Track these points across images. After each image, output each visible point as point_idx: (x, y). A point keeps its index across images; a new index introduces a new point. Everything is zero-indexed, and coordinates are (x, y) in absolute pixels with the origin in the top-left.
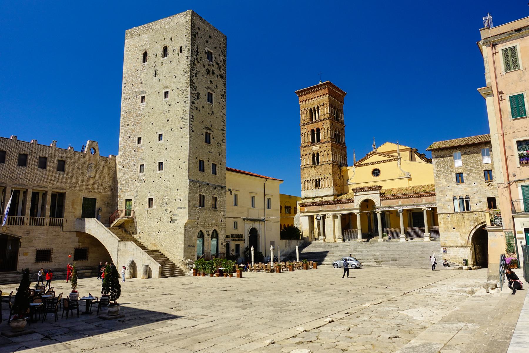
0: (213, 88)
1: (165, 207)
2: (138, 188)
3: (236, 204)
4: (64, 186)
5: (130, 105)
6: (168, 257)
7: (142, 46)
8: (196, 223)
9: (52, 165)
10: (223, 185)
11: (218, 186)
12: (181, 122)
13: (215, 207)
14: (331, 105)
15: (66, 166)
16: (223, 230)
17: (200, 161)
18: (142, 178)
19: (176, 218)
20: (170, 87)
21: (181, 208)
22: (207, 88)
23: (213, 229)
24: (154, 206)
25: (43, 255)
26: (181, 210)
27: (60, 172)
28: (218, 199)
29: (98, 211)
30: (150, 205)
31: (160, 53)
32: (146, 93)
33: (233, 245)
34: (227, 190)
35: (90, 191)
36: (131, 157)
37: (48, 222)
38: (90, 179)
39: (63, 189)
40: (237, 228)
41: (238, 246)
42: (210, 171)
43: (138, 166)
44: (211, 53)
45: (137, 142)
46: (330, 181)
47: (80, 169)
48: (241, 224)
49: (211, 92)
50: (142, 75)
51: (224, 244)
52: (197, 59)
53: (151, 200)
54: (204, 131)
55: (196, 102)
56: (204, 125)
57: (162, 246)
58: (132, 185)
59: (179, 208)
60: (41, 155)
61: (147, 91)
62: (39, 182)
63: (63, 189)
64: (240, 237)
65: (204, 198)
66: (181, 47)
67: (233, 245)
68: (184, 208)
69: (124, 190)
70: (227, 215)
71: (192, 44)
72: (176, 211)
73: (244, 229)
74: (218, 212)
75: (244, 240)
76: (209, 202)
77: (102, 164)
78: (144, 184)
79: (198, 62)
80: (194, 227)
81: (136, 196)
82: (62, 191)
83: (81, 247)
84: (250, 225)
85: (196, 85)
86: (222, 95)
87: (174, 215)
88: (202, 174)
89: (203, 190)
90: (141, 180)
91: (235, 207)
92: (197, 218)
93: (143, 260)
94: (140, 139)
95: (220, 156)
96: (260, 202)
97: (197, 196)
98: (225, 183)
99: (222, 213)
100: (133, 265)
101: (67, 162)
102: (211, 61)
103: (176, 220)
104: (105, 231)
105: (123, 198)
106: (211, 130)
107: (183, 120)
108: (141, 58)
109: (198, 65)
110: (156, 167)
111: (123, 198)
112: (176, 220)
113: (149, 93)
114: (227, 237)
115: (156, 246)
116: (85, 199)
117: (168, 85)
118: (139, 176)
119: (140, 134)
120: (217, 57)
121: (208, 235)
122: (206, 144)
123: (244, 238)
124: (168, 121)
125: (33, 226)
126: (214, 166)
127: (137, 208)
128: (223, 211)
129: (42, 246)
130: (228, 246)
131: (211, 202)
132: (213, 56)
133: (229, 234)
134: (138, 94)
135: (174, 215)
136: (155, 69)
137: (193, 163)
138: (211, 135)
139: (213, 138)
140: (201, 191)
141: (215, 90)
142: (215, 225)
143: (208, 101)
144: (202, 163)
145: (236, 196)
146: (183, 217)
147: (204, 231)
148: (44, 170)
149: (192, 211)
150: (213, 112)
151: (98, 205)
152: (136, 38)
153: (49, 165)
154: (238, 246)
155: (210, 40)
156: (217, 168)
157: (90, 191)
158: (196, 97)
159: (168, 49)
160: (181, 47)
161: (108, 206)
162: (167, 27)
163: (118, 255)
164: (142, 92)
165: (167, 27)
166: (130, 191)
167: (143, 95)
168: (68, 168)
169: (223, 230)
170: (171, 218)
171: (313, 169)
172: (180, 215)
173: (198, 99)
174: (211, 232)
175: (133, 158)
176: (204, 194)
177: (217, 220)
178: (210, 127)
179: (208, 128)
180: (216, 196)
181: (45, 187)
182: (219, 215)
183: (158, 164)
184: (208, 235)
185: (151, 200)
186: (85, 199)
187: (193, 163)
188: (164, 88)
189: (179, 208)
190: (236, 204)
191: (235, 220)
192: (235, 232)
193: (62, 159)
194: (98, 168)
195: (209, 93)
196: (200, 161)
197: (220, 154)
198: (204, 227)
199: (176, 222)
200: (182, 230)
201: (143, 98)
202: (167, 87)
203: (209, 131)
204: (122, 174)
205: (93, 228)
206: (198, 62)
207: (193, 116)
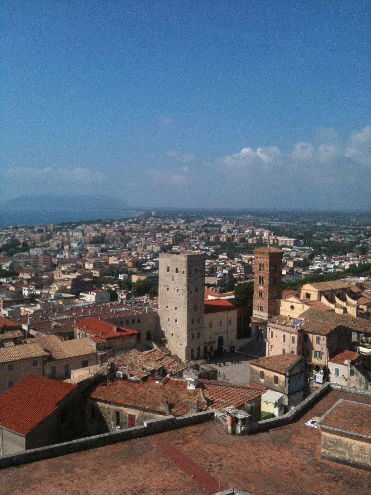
2: (167, 327)
13: (198, 336)
14: (271, 264)
31: (175, 270)
33: (209, 347)
41: (211, 347)
46: (267, 309)
64: (213, 342)
67: (209, 347)
71: (188, 271)
72: (183, 341)
73: (216, 339)
76: (196, 336)
84: (218, 337)
96: (225, 323)
97: (191, 335)
133: (207, 342)
144: (193, 320)
146: (185, 344)
154: (211, 347)
168: (141, 321)
171: (259, 299)
192: (211, 340)
200: (185, 349)
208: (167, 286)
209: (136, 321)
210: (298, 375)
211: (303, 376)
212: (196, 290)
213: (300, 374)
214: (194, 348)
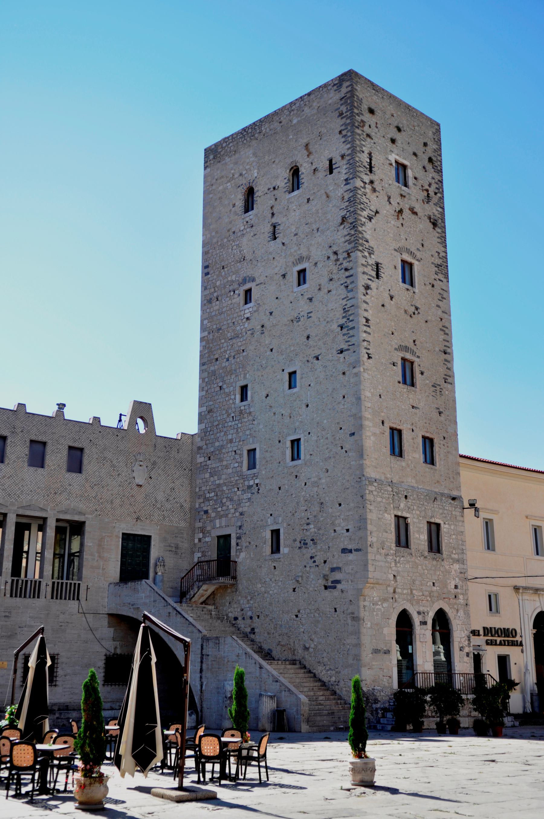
0: (413, 249)
1: (311, 550)
3: (490, 545)
4: (82, 506)
5: (221, 314)
6: (325, 679)
7: (241, 175)
8: (391, 590)
9: (57, 457)
10: (455, 493)
11: (442, 495)
12: (340, 337)
15: (85, 461)
16: (461, 613)
17: (392, 429)
18: (251, 483)
19: (337, 576)
20: (308, 258)
21: (350, 551)
22: (399, 250)
23: (436, 608)
24: (284, 550)
27: (74, 475)
28: (444, 528)
29: (156, 565)
30: (276, 548)
32: (253, 280)
34: (466, 505)
35: (138, 519)
36: (226, 434)
37: (49, 589)
38: (136, 488)
39: (80, 513)
40: (497, 611)
41: (503, 661)
42: (419, 456)
43: (241, 455)
44: (405, 167)
45: (238, 397)
47: (113, 466)
48: (507, 599)
49: (409, 259)
50: (245, 240)
51: (467, 650)
53: (276, 533)
54: (397, 357)
55: (373, 285)
56: (395, 342)
57: (306, 649)
58: (231, 500)
59: (345, 551)
60: (34, 438)
61: (256, 275)
62: (29, 498)
63: (80, 513)
64: (508, 636)
65: (407, 525)
66: (331, 161)
68: (357, 550)
69: (213, 515)
70: (471, 574)
74: (445, 563)
75: (521, 644)
76: (419, 537)
77: (162, 454)
78: (256, 496)
79: (374, 190)
80: (385, 600)
81: (240, 527)
82: (76, 518)
83: (119, 651)
85: (372, 243)
86: (438, 266)
87: (333, 570)
88: (396, 462)
89: (402, 505)
90: (250, 487)
91: (489, 555)
92: (392, 577)
94: (244, 389)
95: (442, 418)
98: (458, 488)
99: (456, 566)
101: (87, 451)
102: (406, 185)
103: (338, 582)
104: (171, 610)
105: (209, 532)
106: (413, 353)
107: (345, 331)
108: (240, 203)
109: (373, 197)
110: (284, 454)
111: (209, 532)
112: (338, 582)
113: (262, 279)
114: (475, 633)
115: (293, 651)
116: (126, 537)
117: (305, 254)
118: (244, 478)
119: (245, 378)
120: (420, 174)
121: (424, 623)
122: (404, 388)
123: (518, 638)
124: (308, 337)
125: (18, 599)
126: (428, 443)
127: (243, 555)
128: (458, 561)
130: (477, 659)
131: (424, 537)
132: (410, 173)
134: (236, 286)
135: (333, 570)
136: (274, 220)
137: (374, 434)
138: (416, 365)
139: (422, 373)
140: (398, 508)
141: (419, 255)
142: (439, 598)
143: (404, 281)
144: (396, 434)
145: (488, 524)
147: (413, 612)
148: (40, 470)
149: (378, 557)
150: (417, 309)
151: (155, 553)
152: (227, 159)
153: (49, 460)
154: (503, 661)
155: (398, 136)
156: (436, 448)
157: (138, 519)
158: (374, 274)
159: (302, 170)
160: (331, 161)
161: (176, 553)
162: (295, 121)
163: (201, 671)
164: (245, 281)
165: (295, 121)
166: (226, 516)
167: (247, 286)
169: (461, 613)
170: (325, 577)
172: (348, 569)
173: (378, 276)
174: (432, 614)
175: (230, 437)
176: (405, 514)
177: (445, 585)
178: (411, 345)
179: (406, 349)
180: (438, 521)
181: (42, 509)
182: (449, 572)
183: (289, 444)
184: (424, 623)
185: (276, 533)
186: (126, 537)
187: (374, 434)
188: (294, 264)
189: (345, 551)
190: (490, 545)
191: (493, 590)
193: (76, 445)
194: (154, 463)
195: (403, 262)
196: (392, 429)
197: (440, 413)
198: (411, 602)
199: (339, 586)
201: (248, 292)
202: (301, 259)
203: (408, 356)
204: (207, 475)
205: (145, 604)
206: (374, 190)
207: (367, 320)
209: (57, 457)
214: (416, 620)
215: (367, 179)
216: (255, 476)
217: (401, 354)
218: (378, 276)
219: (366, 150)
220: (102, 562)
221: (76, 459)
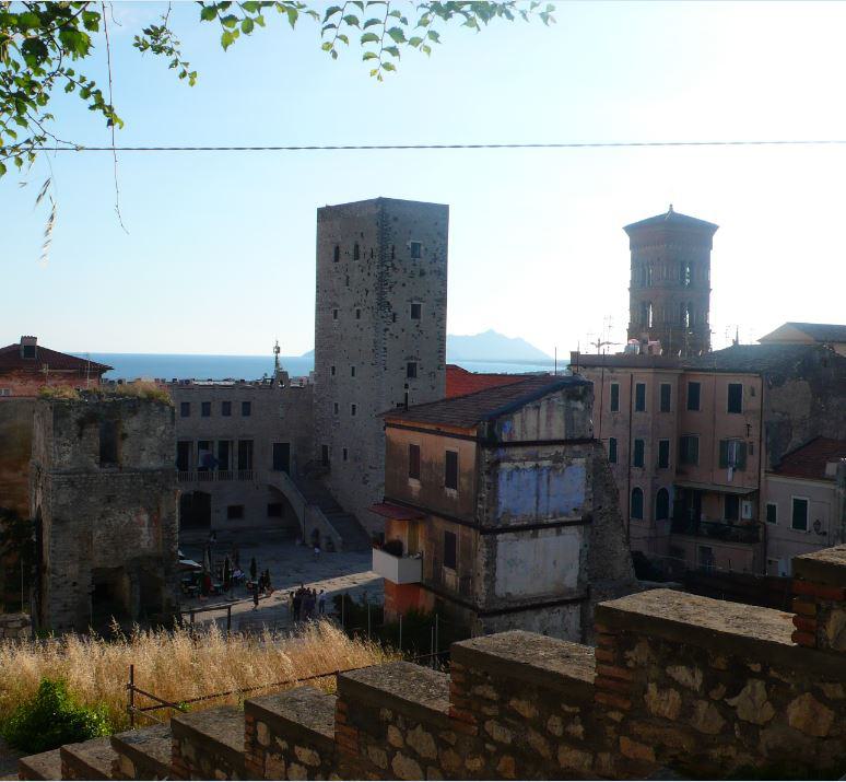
24: (349, 460)
25: (235, 512)
26: (372, 471)
30: (345, 458)
32: (338, 306)
52: (393, 265)
53: (345, 451)
59: (371, 467)
93: (326, 527)
100: (316, 533)
129: (232, 503)
132: (422, 248)
151: (292, 451)
178: (414, 354)
185: (345, 451)
189: (371, 467)
208: (335, 304)
210: (551, 451)
211: (580, 461)
212: (415, 312)
213: (560, 449)
215: (389, 264)
216: (337, 418)
217: (407, 362)
218: (394, 321)
219: (390, 246)
220: (263, 461)
221: (246, 408)
